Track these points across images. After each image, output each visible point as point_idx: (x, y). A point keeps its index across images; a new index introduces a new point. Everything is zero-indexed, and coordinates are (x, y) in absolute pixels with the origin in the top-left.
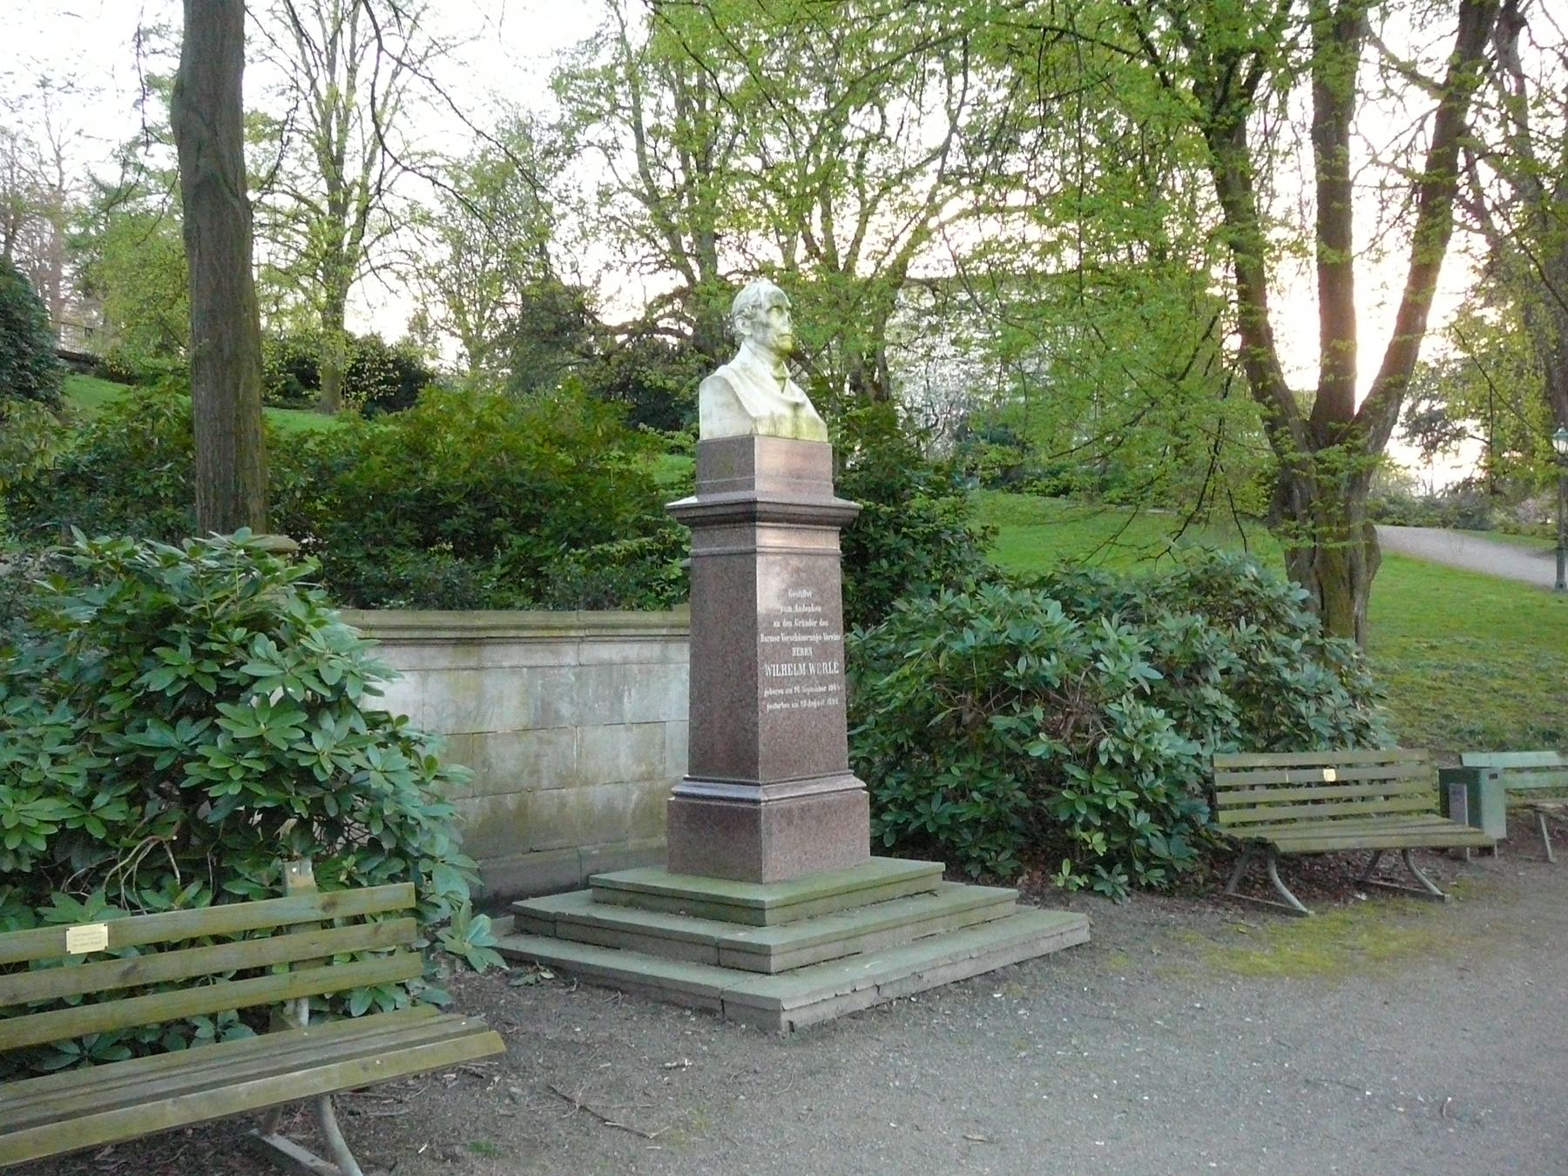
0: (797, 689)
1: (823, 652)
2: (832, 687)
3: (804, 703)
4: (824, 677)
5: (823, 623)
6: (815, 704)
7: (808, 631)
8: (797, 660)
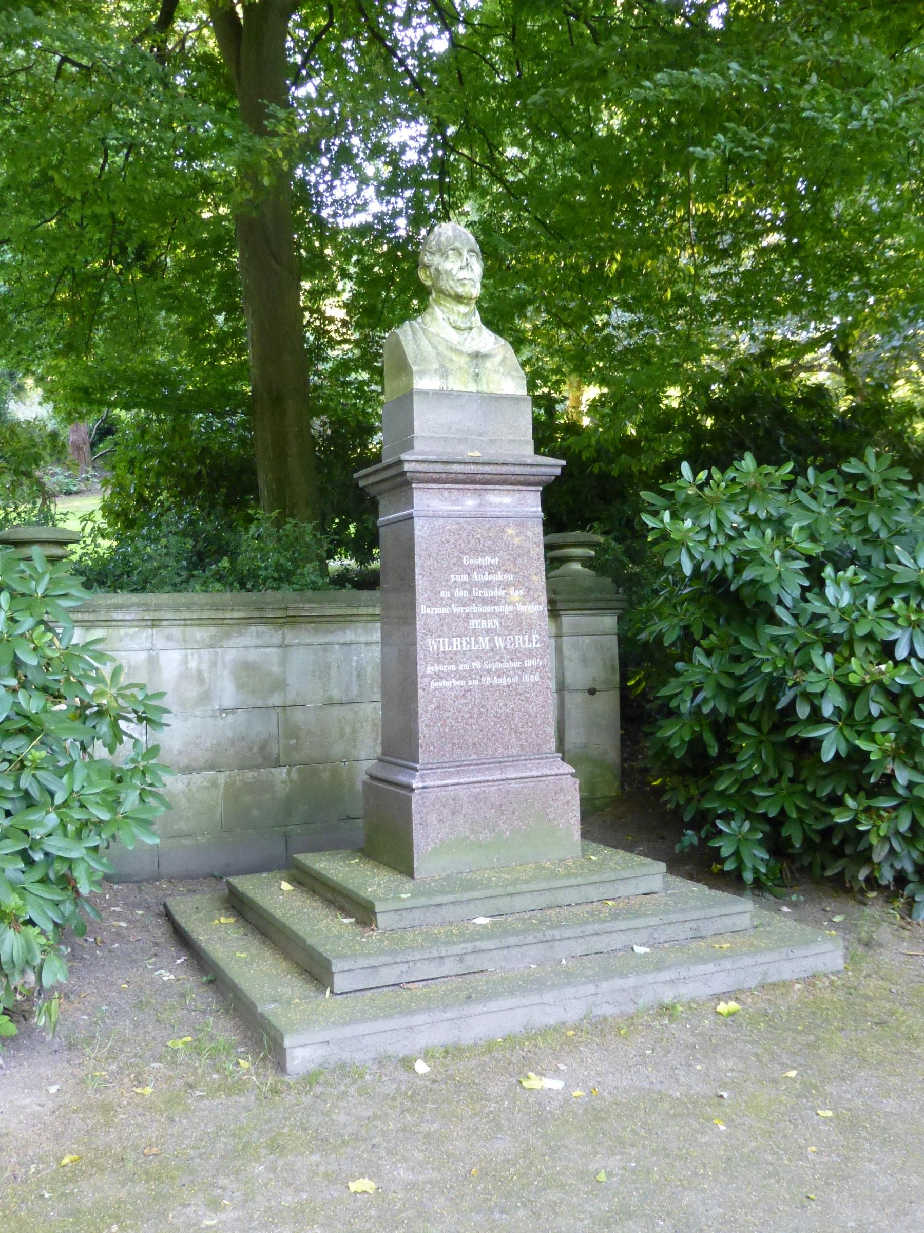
0: (477, 664)
2: (529, 663)
3: (487, 680)
6: (504, 681)
7: (493, 601)
8: (475, 633)
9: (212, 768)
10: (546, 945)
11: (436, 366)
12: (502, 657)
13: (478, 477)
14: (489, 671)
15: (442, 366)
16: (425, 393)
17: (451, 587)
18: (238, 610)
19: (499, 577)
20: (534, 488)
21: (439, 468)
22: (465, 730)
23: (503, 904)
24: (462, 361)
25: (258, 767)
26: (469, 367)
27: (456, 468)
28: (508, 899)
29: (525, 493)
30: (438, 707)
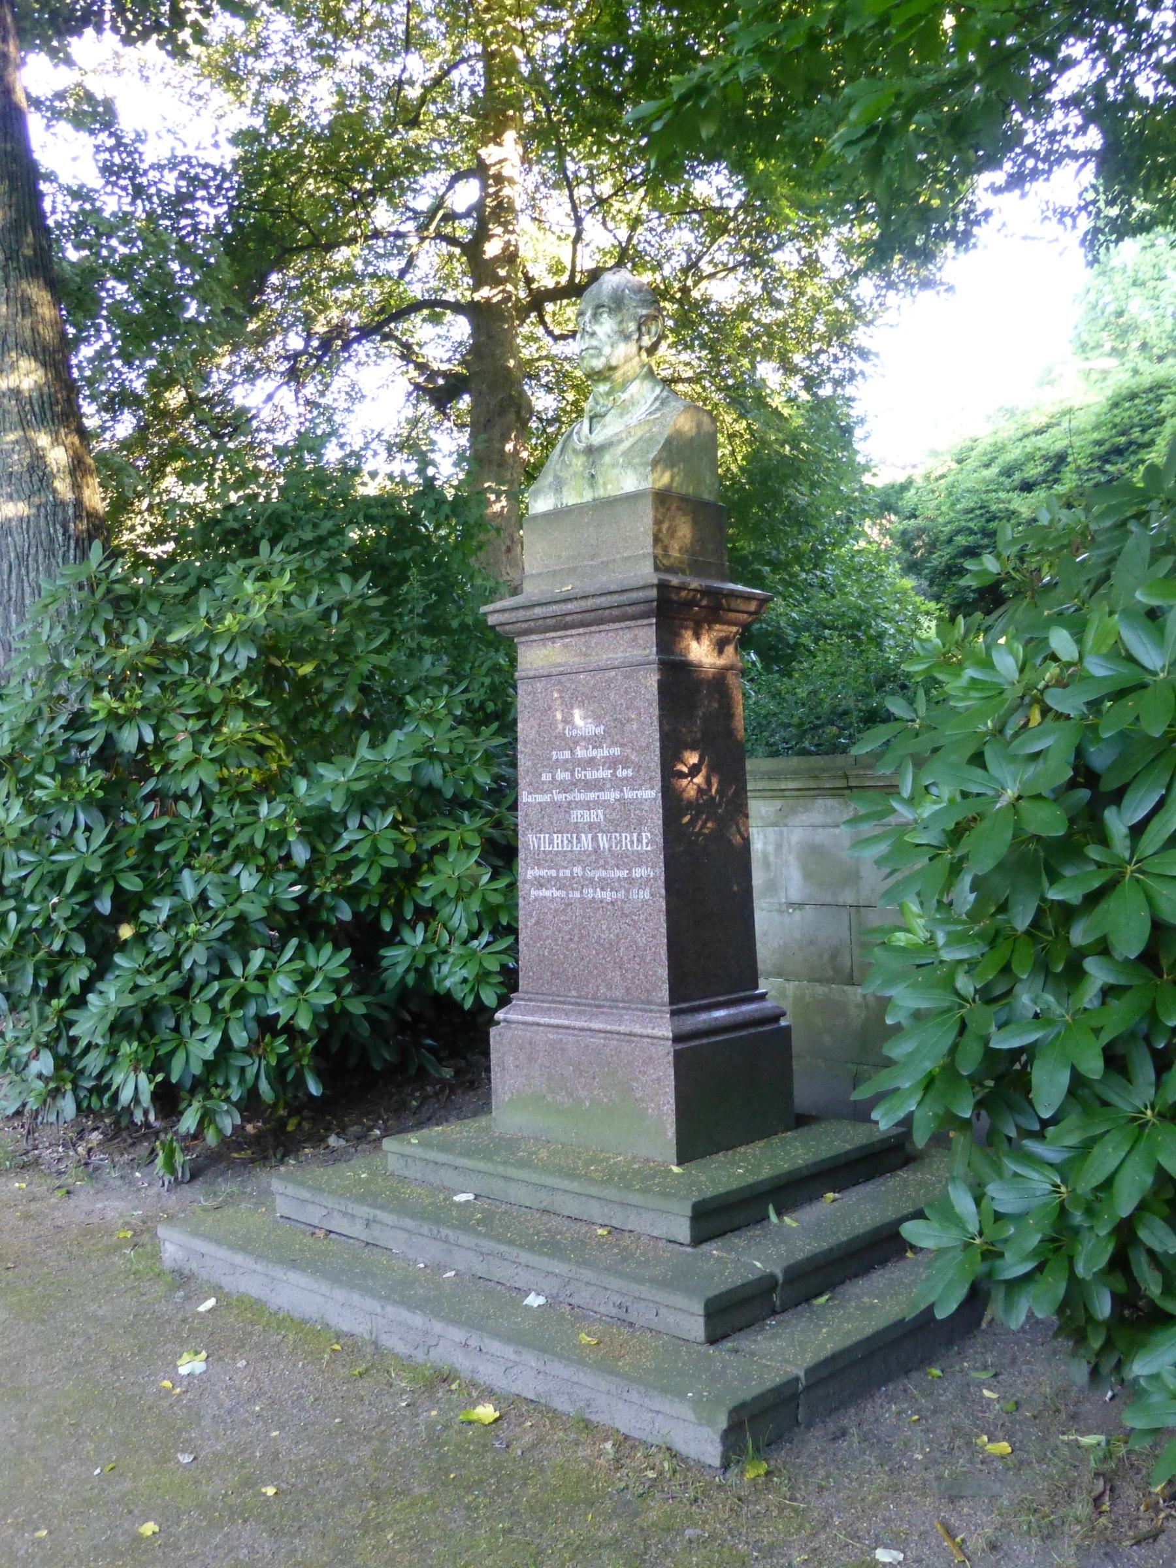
1: (623, 817)
2: (638, 872)
4: (624, 855)
5: (621, 773)
6: (607, 895)
7: (597, 785)
8: (577, 829)
9: (779, 975)
10: (445, 1246)
11: (550, 479)
12: (606, 862)
13: (568, 618)
14: (592, 880)
15: (556, 477)
16: (535, 517)
17: (553, 766)
18: (794, 779)
19: (604, 752)
20: (645, 622)
21: (521, 614)
22: (566, 956)
23: (497, 1186)
24: (578, 462)
25: (829, 981)
26: (585, 468)
27: (538, 611)
28: (501, 1183)
29: (636, 631)
30: (537, 923)
